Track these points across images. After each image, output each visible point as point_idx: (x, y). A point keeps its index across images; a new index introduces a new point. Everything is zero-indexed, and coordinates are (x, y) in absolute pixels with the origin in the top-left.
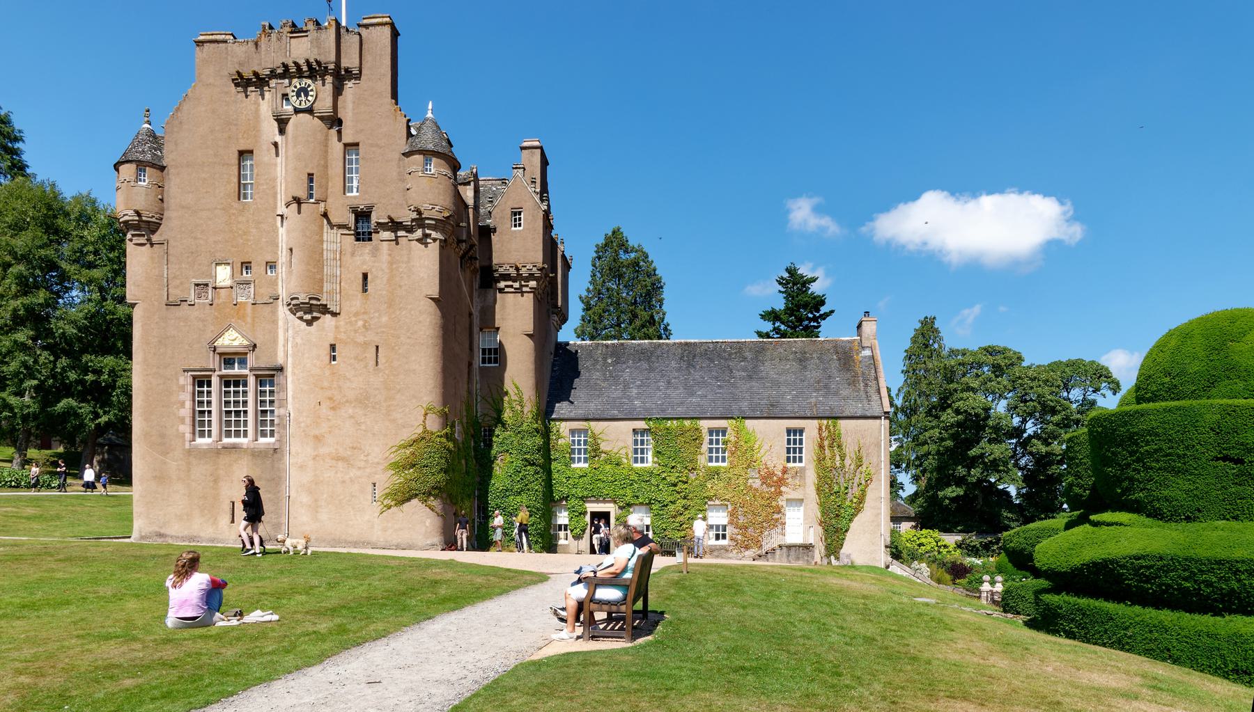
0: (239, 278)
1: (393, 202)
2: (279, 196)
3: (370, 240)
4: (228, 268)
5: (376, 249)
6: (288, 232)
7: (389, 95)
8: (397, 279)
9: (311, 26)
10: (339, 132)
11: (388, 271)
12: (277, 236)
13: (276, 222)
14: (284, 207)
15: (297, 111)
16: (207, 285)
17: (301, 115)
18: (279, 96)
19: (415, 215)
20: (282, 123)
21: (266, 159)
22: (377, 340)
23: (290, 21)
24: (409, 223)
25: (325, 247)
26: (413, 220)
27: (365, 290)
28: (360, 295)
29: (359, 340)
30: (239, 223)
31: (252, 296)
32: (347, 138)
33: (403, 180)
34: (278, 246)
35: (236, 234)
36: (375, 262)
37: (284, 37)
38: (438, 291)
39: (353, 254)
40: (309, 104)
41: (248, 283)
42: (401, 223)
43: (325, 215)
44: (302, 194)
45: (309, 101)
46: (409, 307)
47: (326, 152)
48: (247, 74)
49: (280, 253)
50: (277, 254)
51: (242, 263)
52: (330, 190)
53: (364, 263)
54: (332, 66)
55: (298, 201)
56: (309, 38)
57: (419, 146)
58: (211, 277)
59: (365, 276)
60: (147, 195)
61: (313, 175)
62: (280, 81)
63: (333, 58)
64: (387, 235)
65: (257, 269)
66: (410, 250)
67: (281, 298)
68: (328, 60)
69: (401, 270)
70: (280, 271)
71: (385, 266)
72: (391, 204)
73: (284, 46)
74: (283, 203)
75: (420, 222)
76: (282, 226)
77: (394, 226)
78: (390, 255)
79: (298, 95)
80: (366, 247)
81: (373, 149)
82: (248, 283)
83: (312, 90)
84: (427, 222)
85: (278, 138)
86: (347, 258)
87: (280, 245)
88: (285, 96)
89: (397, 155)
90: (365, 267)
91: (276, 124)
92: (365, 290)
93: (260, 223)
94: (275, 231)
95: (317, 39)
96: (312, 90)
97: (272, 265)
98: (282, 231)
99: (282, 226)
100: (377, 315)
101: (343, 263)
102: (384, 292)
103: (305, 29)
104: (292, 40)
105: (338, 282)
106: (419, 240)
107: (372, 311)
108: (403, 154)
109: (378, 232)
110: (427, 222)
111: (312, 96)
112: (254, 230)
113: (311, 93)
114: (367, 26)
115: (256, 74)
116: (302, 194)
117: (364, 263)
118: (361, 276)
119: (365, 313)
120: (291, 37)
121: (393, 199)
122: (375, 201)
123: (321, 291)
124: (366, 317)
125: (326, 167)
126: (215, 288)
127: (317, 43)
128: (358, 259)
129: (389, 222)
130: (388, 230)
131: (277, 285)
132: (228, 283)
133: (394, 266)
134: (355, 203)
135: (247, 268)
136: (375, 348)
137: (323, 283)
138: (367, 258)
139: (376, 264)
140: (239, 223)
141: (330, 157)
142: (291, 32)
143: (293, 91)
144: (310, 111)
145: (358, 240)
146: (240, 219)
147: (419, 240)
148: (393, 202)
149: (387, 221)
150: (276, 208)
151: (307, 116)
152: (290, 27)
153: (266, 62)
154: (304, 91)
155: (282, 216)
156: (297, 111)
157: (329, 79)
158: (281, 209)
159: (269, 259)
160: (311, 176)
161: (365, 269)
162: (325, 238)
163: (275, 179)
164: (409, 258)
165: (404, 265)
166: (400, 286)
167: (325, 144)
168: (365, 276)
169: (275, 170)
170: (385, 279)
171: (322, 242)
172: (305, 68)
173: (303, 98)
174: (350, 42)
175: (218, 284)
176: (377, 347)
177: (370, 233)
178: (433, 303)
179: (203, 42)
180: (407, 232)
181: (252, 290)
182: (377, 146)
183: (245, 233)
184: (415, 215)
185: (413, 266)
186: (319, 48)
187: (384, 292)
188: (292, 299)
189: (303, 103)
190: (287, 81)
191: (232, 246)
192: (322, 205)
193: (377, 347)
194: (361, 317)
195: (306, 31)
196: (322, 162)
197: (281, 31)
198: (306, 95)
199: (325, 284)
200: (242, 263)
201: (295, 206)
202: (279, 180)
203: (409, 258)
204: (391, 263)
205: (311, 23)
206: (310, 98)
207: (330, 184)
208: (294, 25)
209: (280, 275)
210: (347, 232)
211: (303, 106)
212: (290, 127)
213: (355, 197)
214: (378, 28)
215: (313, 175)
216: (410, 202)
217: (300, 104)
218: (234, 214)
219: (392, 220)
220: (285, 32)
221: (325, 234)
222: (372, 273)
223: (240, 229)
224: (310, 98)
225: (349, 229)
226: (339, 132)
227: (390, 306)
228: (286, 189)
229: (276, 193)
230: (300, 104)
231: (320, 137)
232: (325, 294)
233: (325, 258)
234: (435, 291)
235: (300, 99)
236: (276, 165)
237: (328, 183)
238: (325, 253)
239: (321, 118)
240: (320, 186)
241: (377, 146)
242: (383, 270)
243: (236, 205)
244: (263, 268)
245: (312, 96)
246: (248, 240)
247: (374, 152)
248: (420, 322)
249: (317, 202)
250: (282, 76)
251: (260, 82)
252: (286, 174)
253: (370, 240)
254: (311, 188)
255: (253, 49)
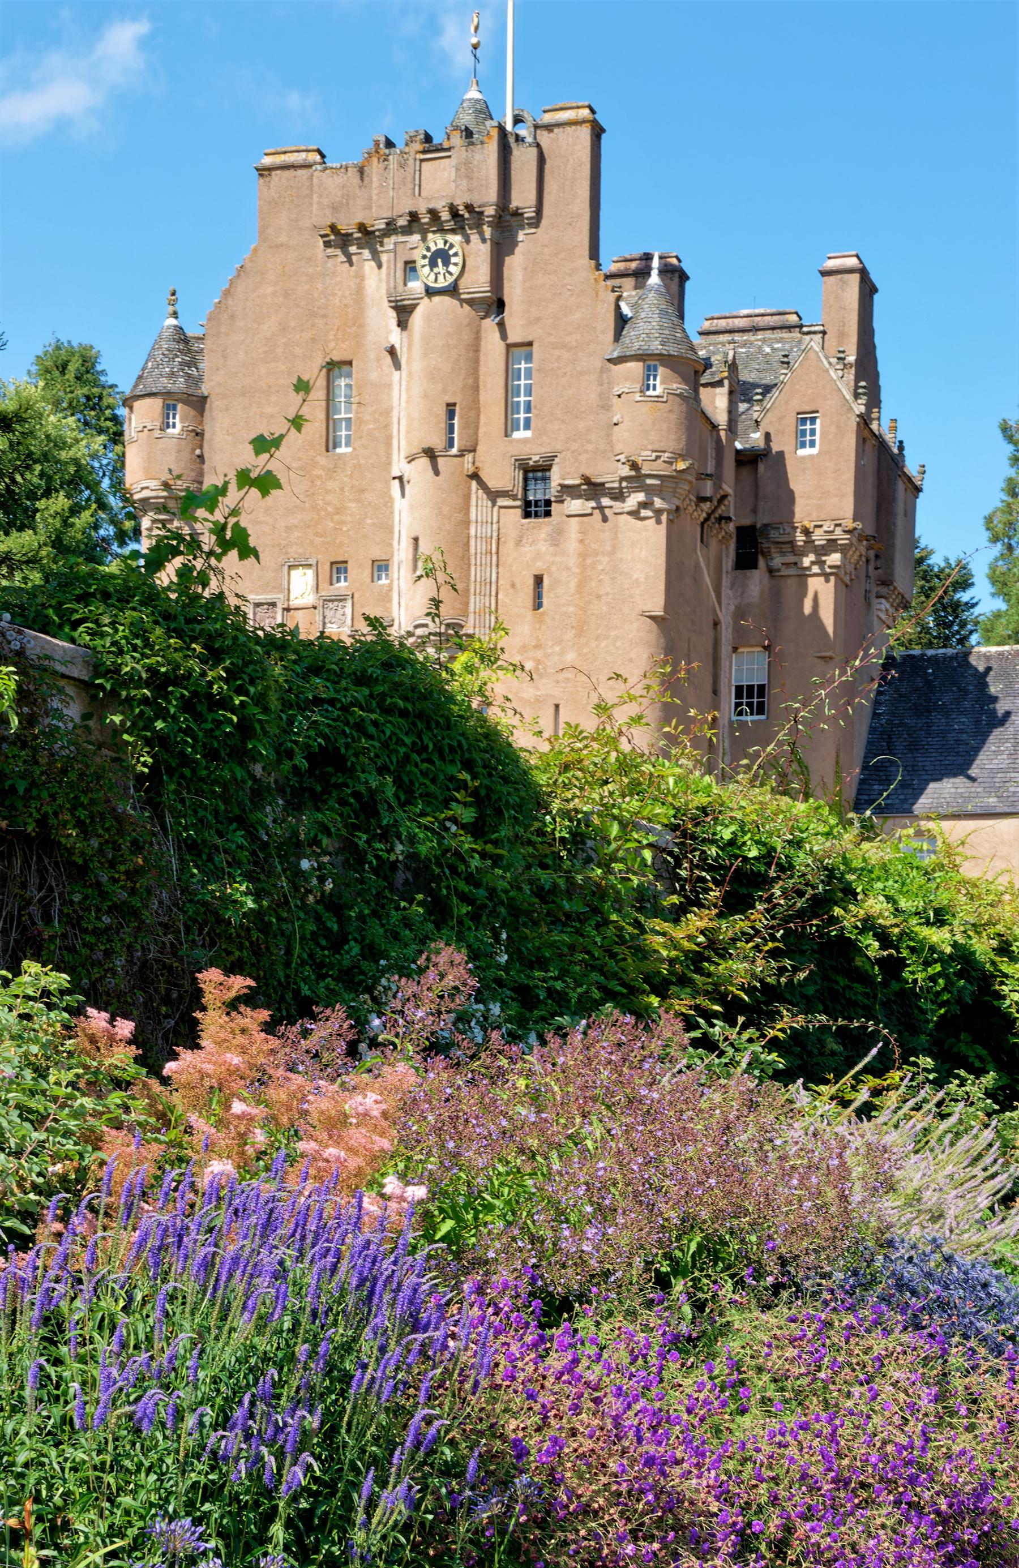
0: (327, 591)
1: (590, 447)
2: (395, 442)
3: (548, 514)
4: (310, 573)
5: (559, 531)
6: (411, 506)
7: (587, 253)
8: (593, 584)
9: (457, 140)
10: (501, 325)
11: (577, 571)
12: (392, 513)
13: (389, 487)
14: (404, 461)
15: (430, 292)
16: (273, 605)
17: (436, 299)
18: (400, 265)
19: (626, 471)
20: (403, 312)
21: (373, 376)
22: (557, 693)
23: (422, 132)
24: (616, 485)
25: (472, 532)
26: (622, 479)
27: (538, 605)
28: (529, 614)
29: (524, 695)
30: (328, 492)
31: (349, 622)
32: (513, 337)
33: (606, 407)
34: (392, 532)
35: (323, 513)
36: (555, 555)
37: (411, 162)
38: (662, 603)
39: (519, 543)
40: (450, 279)
41: (341, 599)
42: (603, 484)
43: (475, 476)
44: (437, 442)
45: (450, 274)
46: (613, 633)
47: (477, 361)
48: (348, 226)
49: (395, 543)
50: (391, 545)
51: (332, 563)
52: (482, 430)
53: (538, 556)
54: (490, 211)
55: (430, 454)
56: (453, 161)
57: (636, 345)
58: (281, 591)
59: (539, 580)
60: (179, 451)
61: (454, 405)
62: (401, 238)
63: (491, 194)
64: (575, 505)
65: (359, 572)
66: (616, 531)
67: (396, 623)
68: (485, 200)
69: (600, 567)
70: (396, 576)
71: (573, 561)
72: (586, 451)
73: (409, 178)
74: (403, 454)
75: (637, 478)
76: (403, 495)
77: (593, 489)
78: (581, 541)
79: (433, 264)
80: (542, 527)
81: (557, 352)
82: (341, 599)
83: (456, 254)
84: (649, 481)
85: (396, 337)
86: (508, 549)
87: (396, 530)
88: (410, 267)
89: (598, 363)
90: (539, 564)
91: (393, 314)
92: (538, 605)
93: (363, 491)
94: (389, 502)
95: (467, 163)
96: (456, 254)
97: (381, 567)
98: (400, 504)
99: (403, 495)
100: (557, 649)
101: (502, 560)
102: (571, 609)
103: (446, 145)
104: (424, 164)
105: (493, 593)
106: (634, 514)
107: (550, 643)
108: (609, 360)
109: (562, 502)
110: (649, 481)
111: (456, 264)
112: (353, 505)
113: (453, 260)
114: (549, 128)
115: (362, 228)
116: (437, 442)
117: (538, 556)
118: (531, 581)
119: (537, 647)
120: (422, 161)
121: (589, 441)
122: (559, 447)
123: (465, 613)
124: (539, 654)
125: (476, 388)
126: (288, 610)
127: (466, 171)
128: (527, 551)
129: (579, 485)
130: (579, 497)
131: (390, 601)
132: (310, 599)
133: (589, 561)
134: (523, 452)
135: (338, 571)
136: (552, 709)
137: (468, 597)
138: (543, 547)
139: (558, 559)
140: (328, 492)
141: (482, 370)
142: (424, 152)
143: (424, 257)
144: (452, 291)
145: (527, 515)
146: (330, 485)
147: (634, 514)
148: (590, 447)
149: (577, 482)
150: (389, 463)
151: (447, 301)
152: (422, 143)
153: (380, 206)
154: (441, 257)
155: (400, 478)
156: (430, 292)
157: (487, 231)
158: (399, 466)
159: (377, 553)
160: (451, 410)
161: (538, 567)
162: (473, 516)
163: (388, 412)
164: (614, 547)
165: (605, 559)
166: (599, 597)
167: (475, 346)
168: (539, 580)
169: (389, 395)
170: (572, 585)
171: (467, 523)
172: (445, 216)
173: (440, 268)
174: (523, 160)
175: (294, 603)
176: (557, 706)
177: (548, 503)
178: (654, 626)
179: (270, 169)
180: (612, 499)
181: (348, 611)
182: (564, 346)
183: (338, 511)
184: (626, 471)
185: (621, 560)
186: (469, 178)
187: (571, 609)
188: (416, 627)
189: (441, 278)
190: (416, 238)
191: (316, 534)
192: (469, 457)
193: (557, 706)
194: (531, 654)
195: (449, 149)
196: (470, 381)
197: (407, 150)
198: (447, 263)
199: (472, 597)
200: (332, 563)
201: (424, 462)
202: (395, 414)
203: (614, 547)
204: (583, 556)
205: (457, 134)
206: (452, 268)
207: (483, 419)
208: (428, 138)
209: (395, 583)
210: (511, 503)
211: (442, 283)
212: (417, 319)
213: (525, 441)
214: (569, 130)
215: (454, 405)
216: (619, 448)
217: (436, 280)
218: (319, 477)
219: (587, 480)
220: (412, 153)
221: (473, 510)
222: (550, 575)
223: (328, 504)
224: (452, 268)
225: (514, 498)
226: (501, 325)
227: (580, 632)
228: (408, 432)
229: (389, 438)
230: (436, 280)
231: (467, 336)
232: (471, 617)
233: (472, 550)
234: (656, 605)
235: (436, 270)
236: (390, 385)
237: (478, 416)
238: (472, 543)
239: (471, 302)
240: (464, 426)
241: (564, 346)
242: (569, 569)
243: (323, 460)
244: (367, 572)
245: (456, 264)
246: (343, 523)
247: (559, 358)
248: (631, 660)
249: (461, 454)
250: (407, 231)
251: (368, 237)
252: (407, 402)
253: (548, 514)
254: (451, 429)
255: (356, 180)
